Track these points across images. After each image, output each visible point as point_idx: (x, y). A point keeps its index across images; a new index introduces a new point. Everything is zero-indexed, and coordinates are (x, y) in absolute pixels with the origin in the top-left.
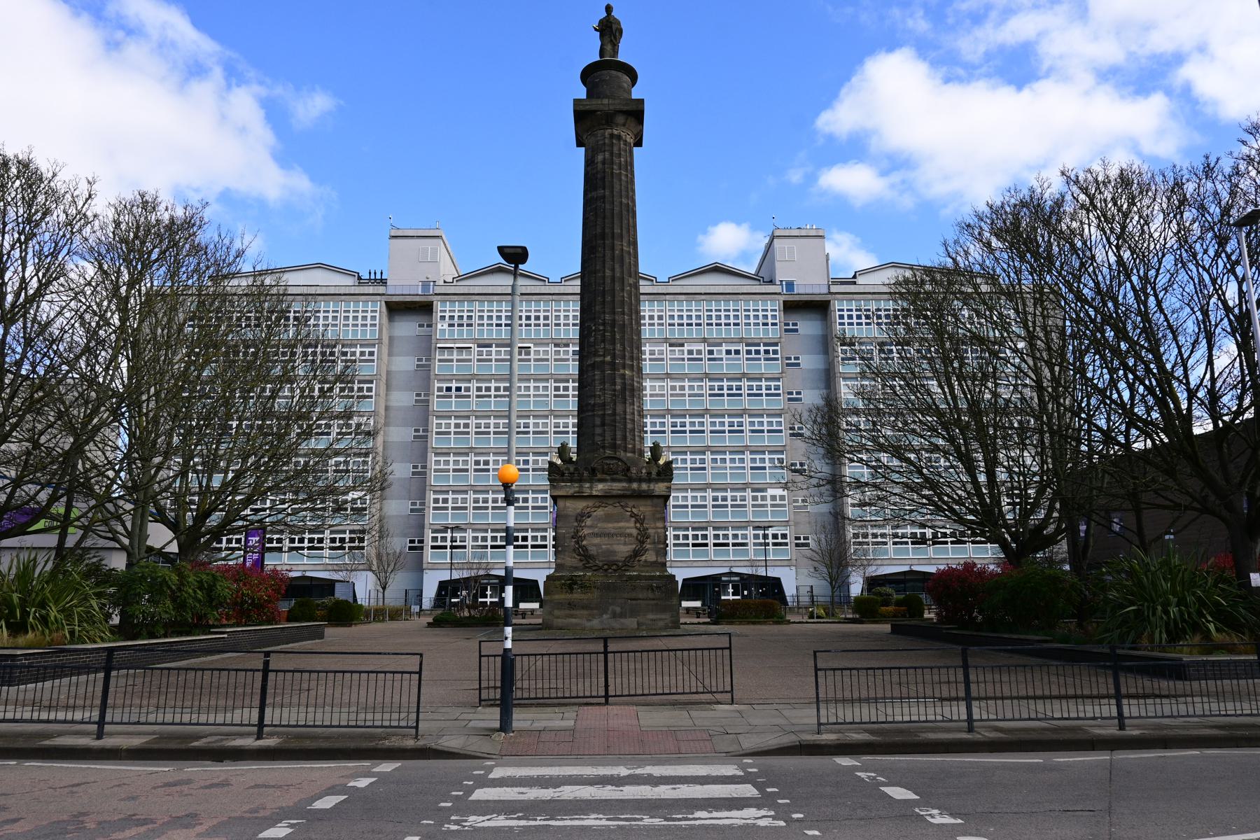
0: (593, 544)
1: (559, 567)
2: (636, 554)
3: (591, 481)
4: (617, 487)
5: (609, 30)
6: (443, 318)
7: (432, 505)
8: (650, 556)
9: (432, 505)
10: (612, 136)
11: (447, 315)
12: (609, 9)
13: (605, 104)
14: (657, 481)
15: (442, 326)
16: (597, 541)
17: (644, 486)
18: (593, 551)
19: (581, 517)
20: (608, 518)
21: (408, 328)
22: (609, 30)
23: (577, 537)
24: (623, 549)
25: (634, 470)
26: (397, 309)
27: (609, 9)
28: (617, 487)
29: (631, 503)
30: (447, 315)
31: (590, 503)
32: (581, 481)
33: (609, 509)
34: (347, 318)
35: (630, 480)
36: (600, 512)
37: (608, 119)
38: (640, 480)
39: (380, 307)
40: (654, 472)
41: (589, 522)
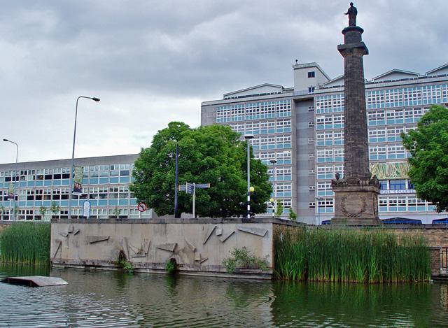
0: (348, 208)
1: (336, 216)
2: (362, 211)
3: (346, 186)
4: (355, 188)
5: (352, 13)
6: (318, 104)
7: (318, 188)
8: (367, 212)
9: (318, 188)
10: (353, 57)
11: (320, 103)
12: (352, 4)
13: (350, 45)
14: (369, 185)
15: (318, 108)
16: (348, 207)
17: (364, 187)
18: (347, 210)
19: (343, 199)
20: (352, 199)
21: (304, 109)
22: (352, 13)
23: (343, 206)
24: (358, 210)
25: (361, 182)
26: (299, 102)
27: (352, 4)
28: (355, 188)
29: (360, 193)
30: (320, 103)
31: (346, 194)
32: (343, 186)
33: (353, 196)
34: (278, 108)
35: (359, 186)
36: (350, 197)
37: (351, 51)
38: (363, 186)
39: (292, 102)
40: (368, 182)
41: (346, 200)
